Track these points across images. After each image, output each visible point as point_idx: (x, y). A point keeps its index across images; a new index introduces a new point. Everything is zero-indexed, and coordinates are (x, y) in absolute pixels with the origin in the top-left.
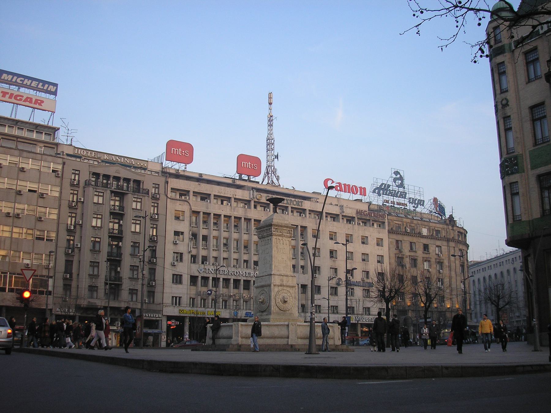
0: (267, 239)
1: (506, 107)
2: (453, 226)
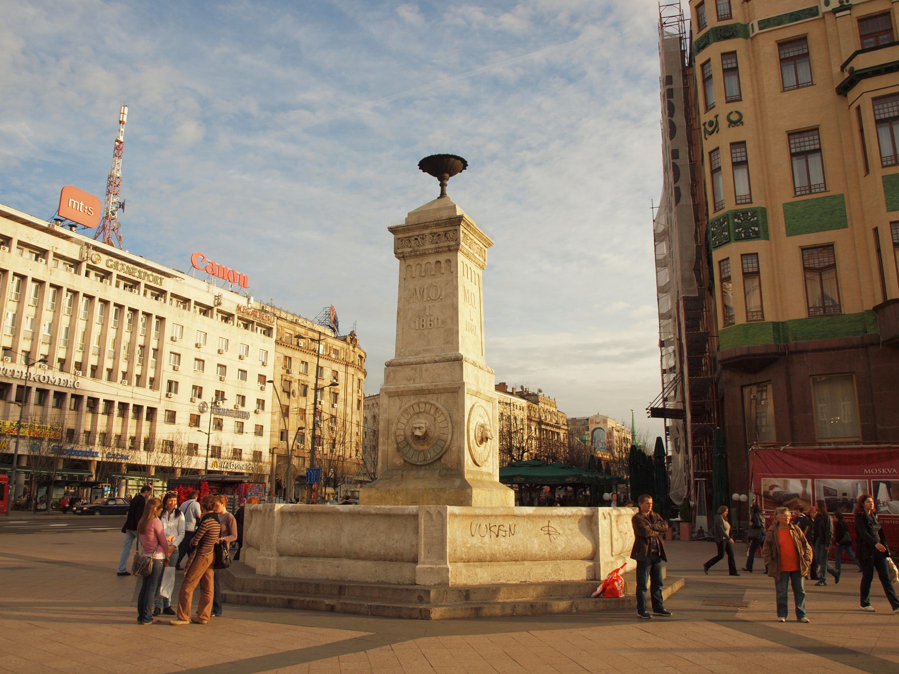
0: (432, 260)
2: (354, 347)
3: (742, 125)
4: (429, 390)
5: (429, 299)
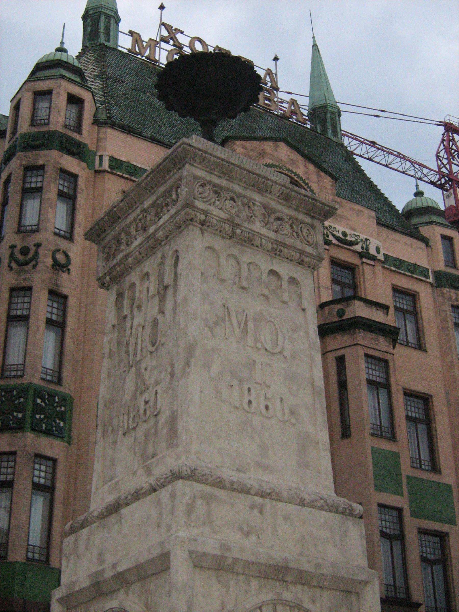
1: (64, 272)
3: (69, 273)
4: (301, 572)
5: (259, 345)
